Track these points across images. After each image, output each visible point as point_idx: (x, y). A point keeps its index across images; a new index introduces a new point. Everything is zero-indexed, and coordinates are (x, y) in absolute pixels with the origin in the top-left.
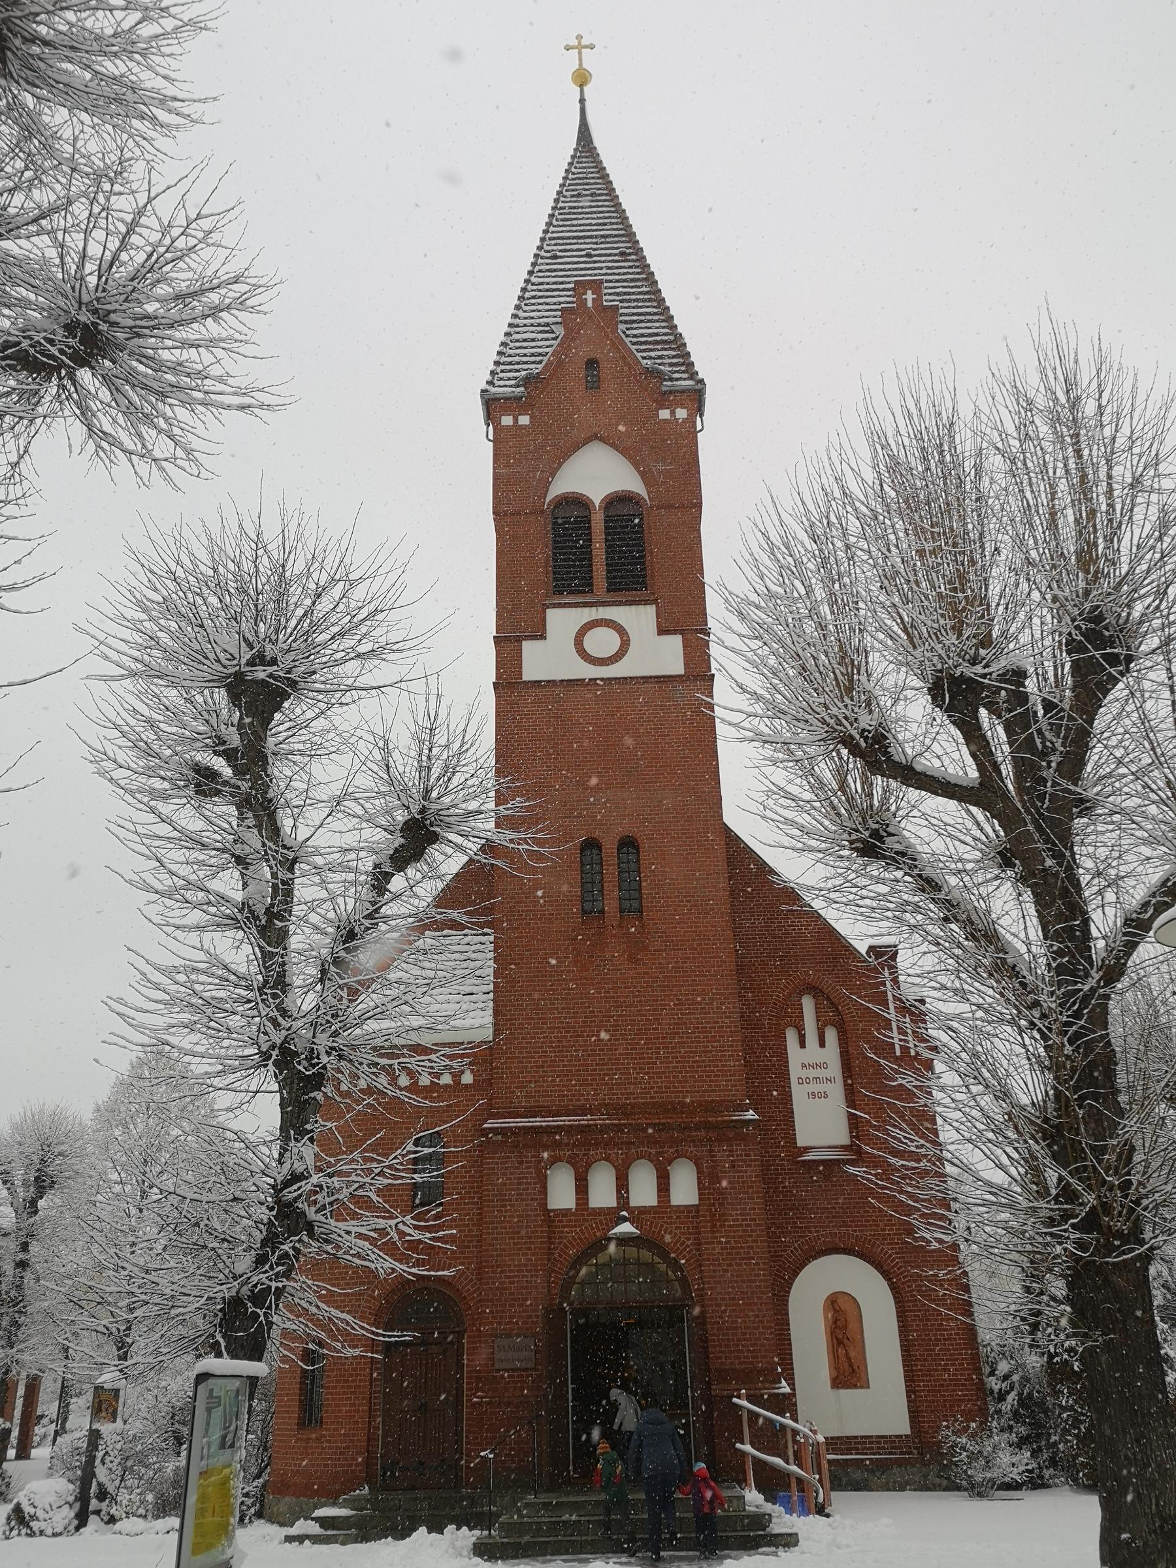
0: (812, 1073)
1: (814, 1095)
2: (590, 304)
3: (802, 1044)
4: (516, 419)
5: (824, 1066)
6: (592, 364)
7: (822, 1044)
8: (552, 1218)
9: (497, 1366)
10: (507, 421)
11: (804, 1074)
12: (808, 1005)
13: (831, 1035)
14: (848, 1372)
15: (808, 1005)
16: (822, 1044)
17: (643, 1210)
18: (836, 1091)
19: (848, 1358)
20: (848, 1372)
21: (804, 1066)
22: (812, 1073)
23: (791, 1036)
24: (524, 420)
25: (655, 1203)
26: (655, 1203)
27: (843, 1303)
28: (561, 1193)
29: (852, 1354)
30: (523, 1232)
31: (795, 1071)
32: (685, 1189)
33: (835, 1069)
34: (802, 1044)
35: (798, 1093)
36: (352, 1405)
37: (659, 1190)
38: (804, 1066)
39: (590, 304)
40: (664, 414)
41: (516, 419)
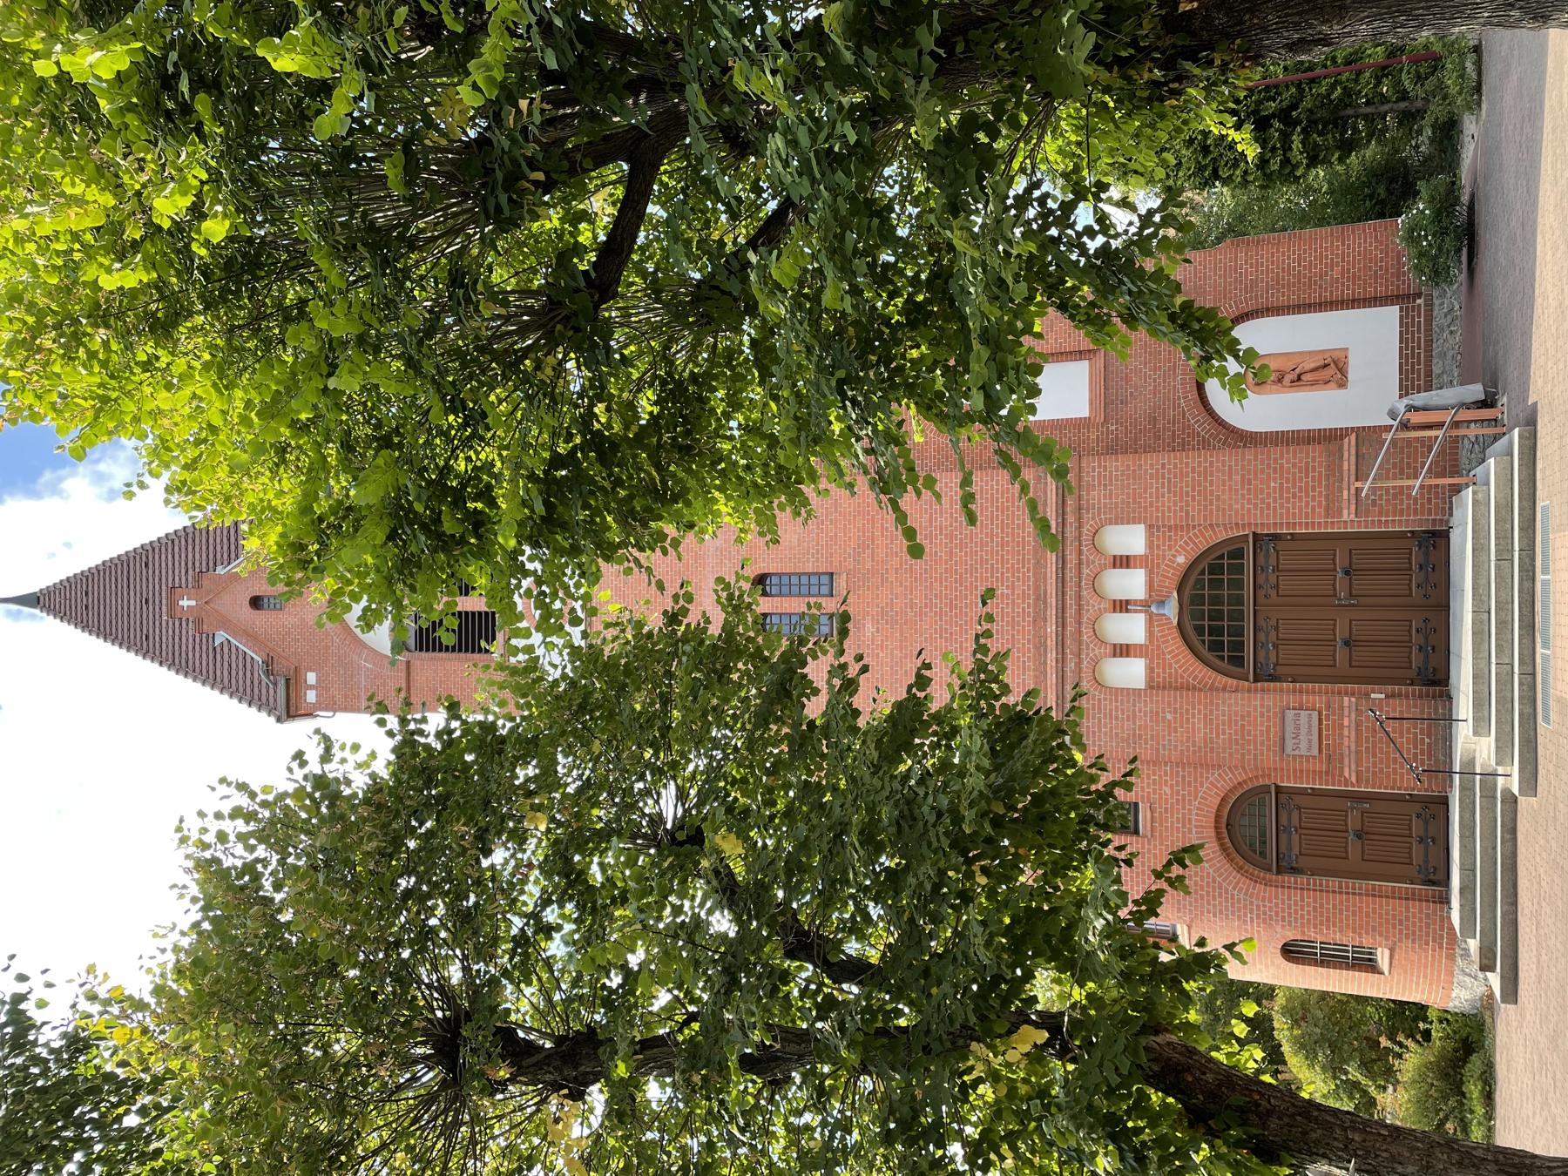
2: (193, 603)
4: (311, 687)
6: (256, 602)
8: (1152, 685)
9: (1315, 752)
10: (311, 696)
14: (1330, 370)
17: (1150, 585)
20: (1330, 370)
24: (311, 678)
25: (1142, 571)
26: (1142, 571)
28: (1130, 673)
30: (1169, 716)
32: (1130, 539)
36: (1354, 914)
37: (1128, 567)
39: (193, 603)
41: (311, 687)
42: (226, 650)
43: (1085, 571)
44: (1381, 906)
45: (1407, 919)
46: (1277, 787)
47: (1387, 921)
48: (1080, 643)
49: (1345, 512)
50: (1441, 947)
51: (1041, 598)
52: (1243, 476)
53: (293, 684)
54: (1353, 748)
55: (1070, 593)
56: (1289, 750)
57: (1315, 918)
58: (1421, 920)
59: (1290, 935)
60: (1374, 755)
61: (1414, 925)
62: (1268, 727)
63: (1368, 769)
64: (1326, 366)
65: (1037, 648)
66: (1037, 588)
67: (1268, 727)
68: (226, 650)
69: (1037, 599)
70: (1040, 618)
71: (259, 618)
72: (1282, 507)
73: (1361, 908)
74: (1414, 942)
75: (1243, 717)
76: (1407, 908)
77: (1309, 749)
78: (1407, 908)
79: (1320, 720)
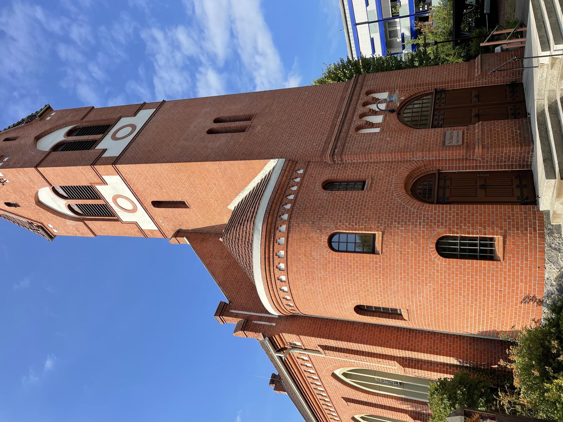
36: (481, 215)
43: (360, 101)
44: (497, 210)
45: (513, 215)
46: (440, 173)
47: (501, 218)
48: (352, 121)
50: (535, 230)
51: (338, 112)
54: (480, 137)
55: (351, 109)
56: (447, 143)
57: (457, 219)
58: (521, 215)
59: (442, 232)
60: (491, 138)
61: (517, 218)
62: (437, 139)
63: (488, 144)
65: (331, 127)
66: (337, 110)
67: (437, 139)
69: (336, 113)
70: (336, 117)
73: (485, 212)
74: (518, 230)
75: (424, 136)
76: (513, 210)
77: (458, 142)
78: (513, 210)
79: (463, 134)
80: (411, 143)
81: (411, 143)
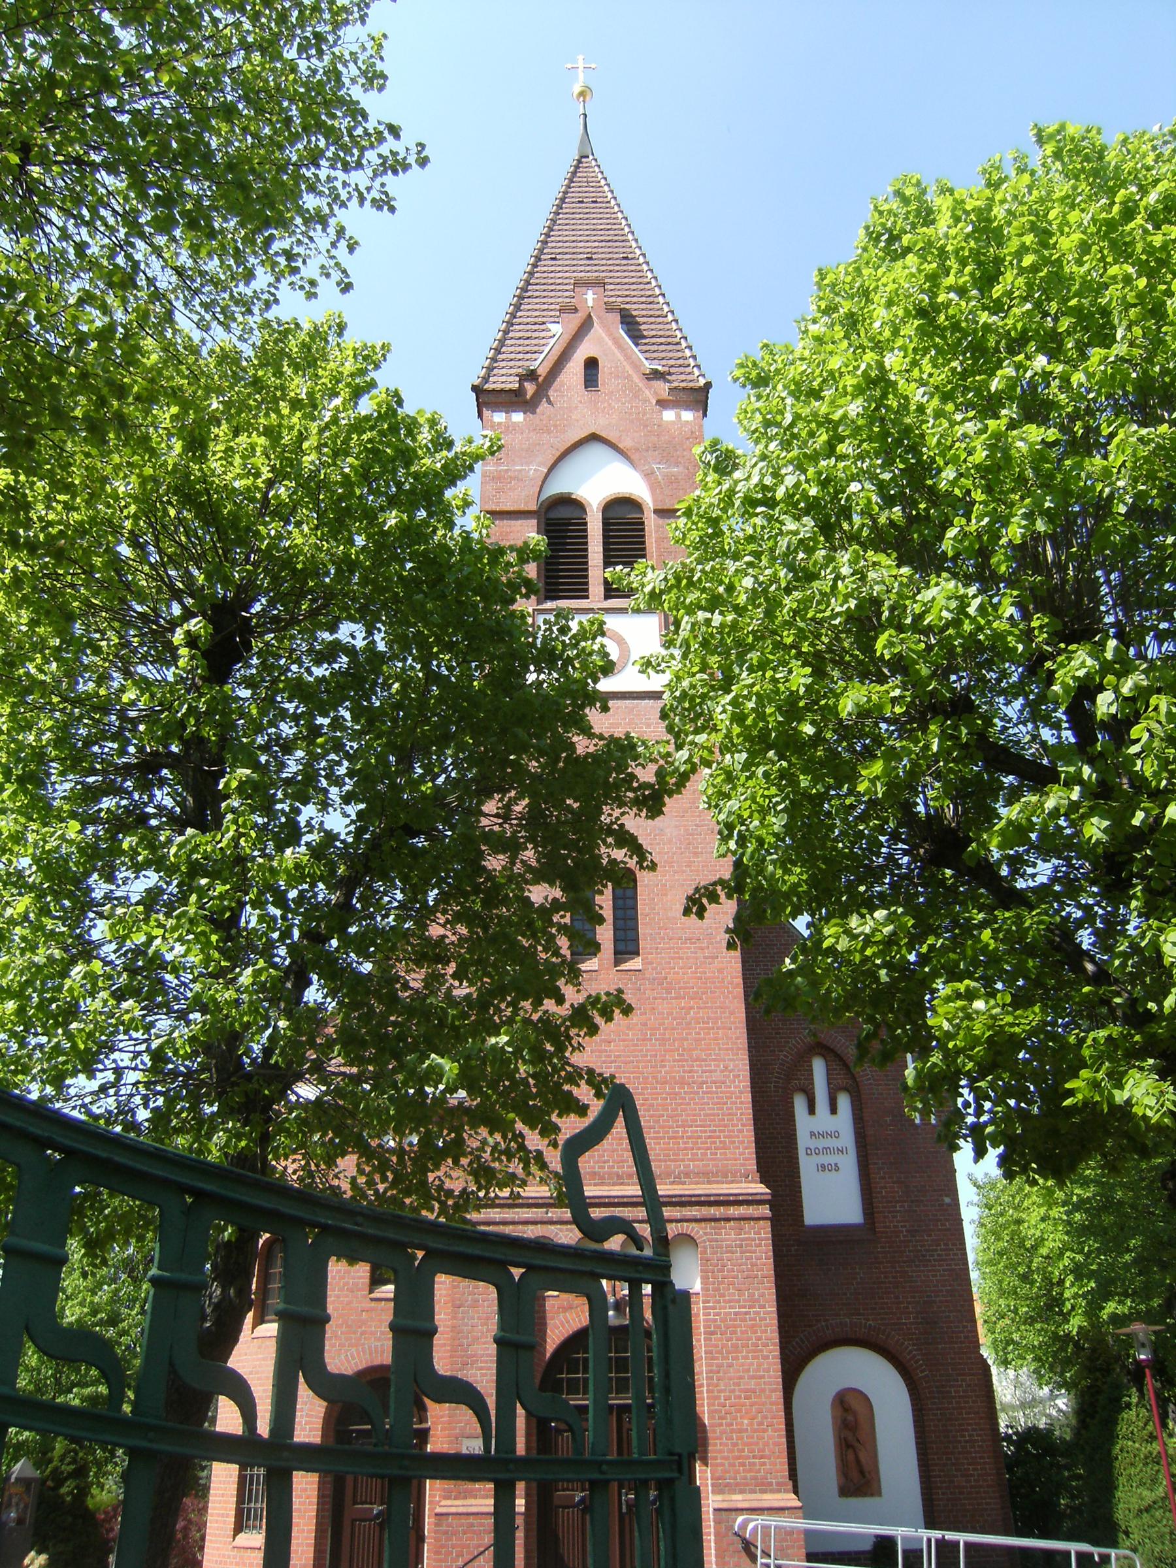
0: (821, 1143)
1: (823, 1166)
2: (590, 303)
3: (812, 1110)
4: (508, 419)
5: (835, 1135)
7: (833, 1110)
10: (499, 417)
11: (813, 1144)
12: (819, 1068)
13: (844, 1102)
15: (819, 1068)
16: (833, 1110)
18: (849, 1164)
19: (858, 1461)
21: (812, 1134)
22: (821, 1143)
23: (799, 1104)
27: (855, 1404)
29: (863, 1456)
31: (803, 1141)
33: (847, 1139)
34: (812, 1110)
35: (807, 1166)
38: (812, 1134)
39: (590, 303)
40: (669, 415)
41: (508, 419)
42: (543, 334)
49: (719, 1497)
52: (754, 1391)
53: (513, 400)
64: (862, 1472)
68: (543, 334)
71: (575, 368)
72: (724, 1432)
80: (481, 1368)
81: (481, 1368)
